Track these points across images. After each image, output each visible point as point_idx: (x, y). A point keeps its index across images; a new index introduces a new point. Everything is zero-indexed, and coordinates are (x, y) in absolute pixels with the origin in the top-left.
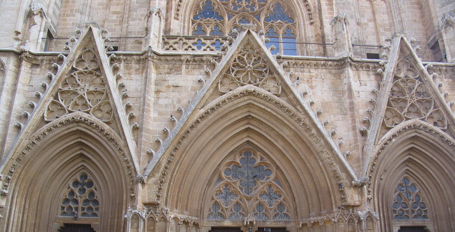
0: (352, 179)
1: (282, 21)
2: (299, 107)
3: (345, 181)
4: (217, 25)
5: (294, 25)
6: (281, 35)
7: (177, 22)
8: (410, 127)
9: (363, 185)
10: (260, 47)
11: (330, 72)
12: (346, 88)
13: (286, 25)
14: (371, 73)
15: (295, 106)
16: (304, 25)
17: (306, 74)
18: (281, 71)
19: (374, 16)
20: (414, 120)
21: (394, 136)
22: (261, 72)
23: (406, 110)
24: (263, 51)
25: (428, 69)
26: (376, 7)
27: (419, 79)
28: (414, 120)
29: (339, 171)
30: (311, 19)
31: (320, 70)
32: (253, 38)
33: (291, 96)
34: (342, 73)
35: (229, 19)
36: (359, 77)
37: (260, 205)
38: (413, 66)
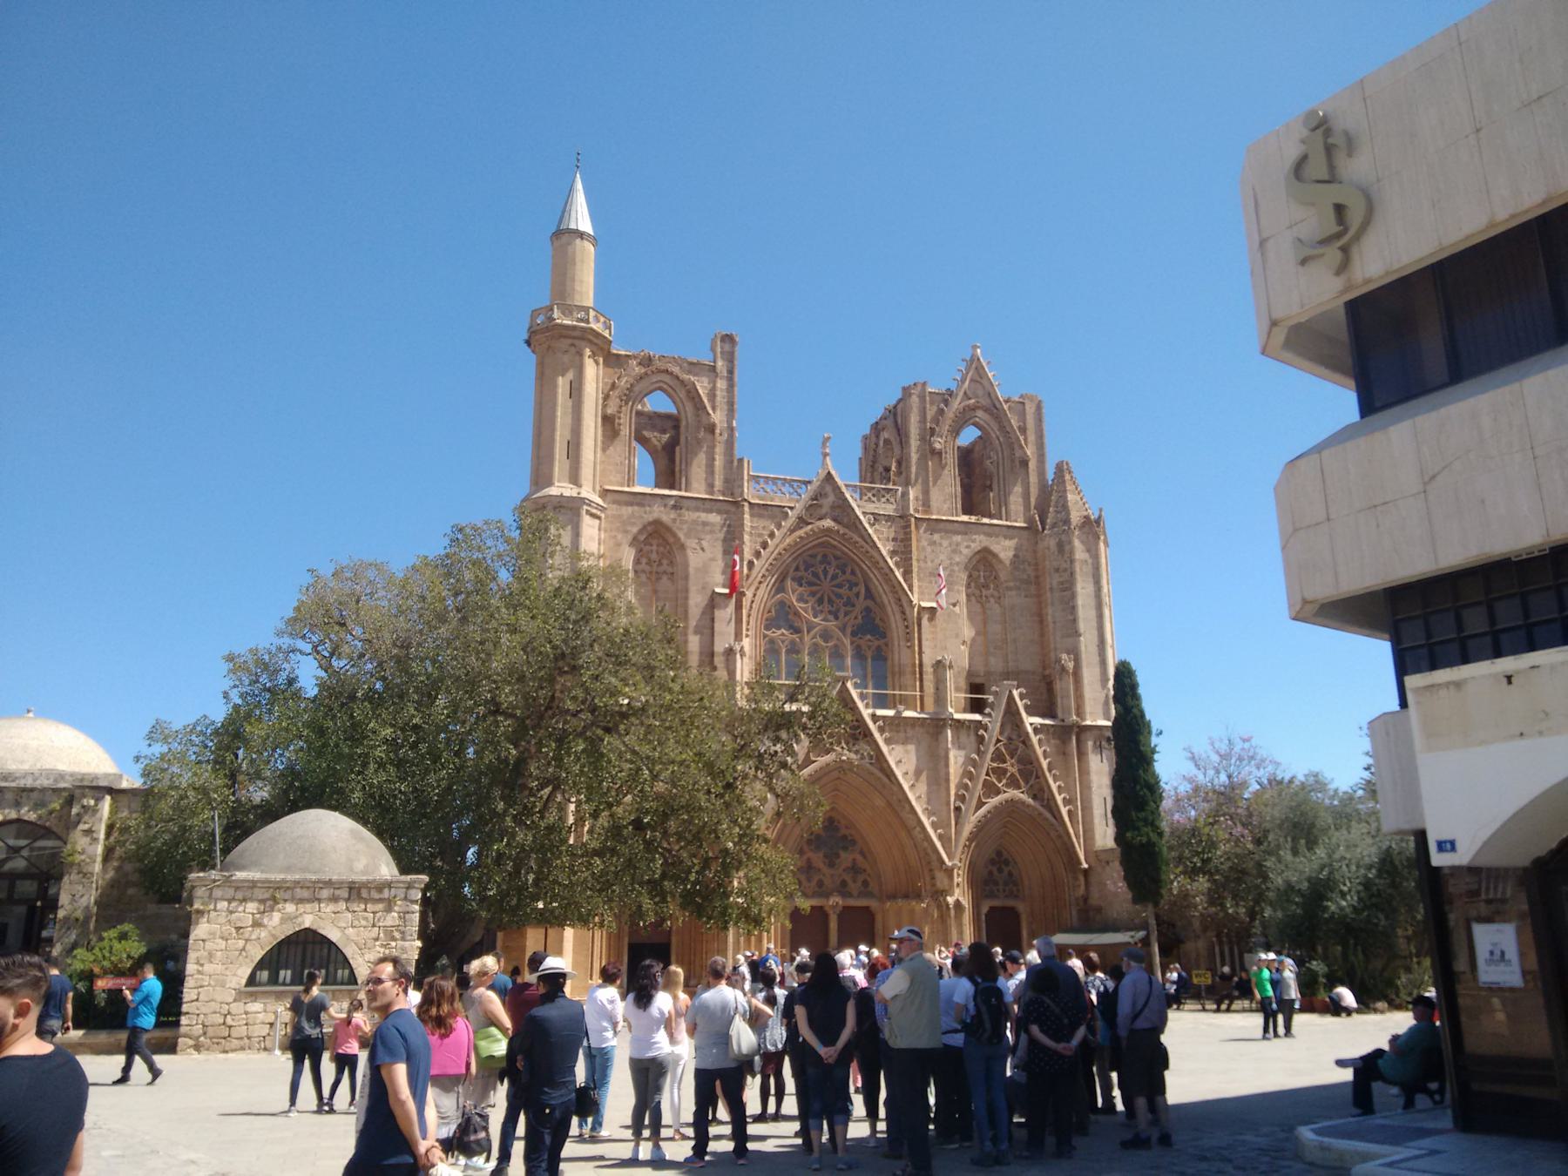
0: (943, 862)
1: (872, 635)
2: (893, 778)
3: (935, 864)
4: (793, 642)
5: (887, 645)
6: (869, 660)
7: (748, 639)
8: (1007, 801)
9: (953, 870)
10: (854, 702)
11: (928, 733)
12: (943, 754)
13: (876, 643)
14: (972, 733)
15: (888, 777)
16: (899, 645)
17: (902, 735)
18: (877, 735)
19: (985, 627)
20: (1013, 793)
21: (989, 812)
22: (854, 734)
23: (1004, 781)
24: (857, 708)
25: (1036, 731)
26: (988, 612)
27: (1024, 742)
28: (1013, 793)
29: (929, 851)
30: (908, 641)
31: (917, 728)
32: (848, 690)
33: (885, 765)
34: (941, 733)
35: (808, 632)
36: (958, 738)
37: (844, 883)
38: (1017, 724)
